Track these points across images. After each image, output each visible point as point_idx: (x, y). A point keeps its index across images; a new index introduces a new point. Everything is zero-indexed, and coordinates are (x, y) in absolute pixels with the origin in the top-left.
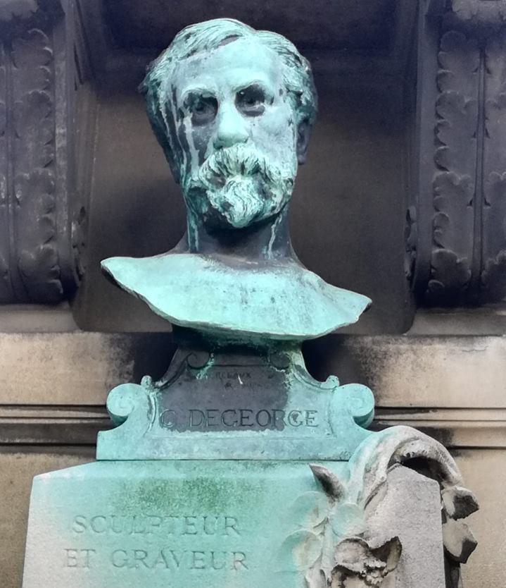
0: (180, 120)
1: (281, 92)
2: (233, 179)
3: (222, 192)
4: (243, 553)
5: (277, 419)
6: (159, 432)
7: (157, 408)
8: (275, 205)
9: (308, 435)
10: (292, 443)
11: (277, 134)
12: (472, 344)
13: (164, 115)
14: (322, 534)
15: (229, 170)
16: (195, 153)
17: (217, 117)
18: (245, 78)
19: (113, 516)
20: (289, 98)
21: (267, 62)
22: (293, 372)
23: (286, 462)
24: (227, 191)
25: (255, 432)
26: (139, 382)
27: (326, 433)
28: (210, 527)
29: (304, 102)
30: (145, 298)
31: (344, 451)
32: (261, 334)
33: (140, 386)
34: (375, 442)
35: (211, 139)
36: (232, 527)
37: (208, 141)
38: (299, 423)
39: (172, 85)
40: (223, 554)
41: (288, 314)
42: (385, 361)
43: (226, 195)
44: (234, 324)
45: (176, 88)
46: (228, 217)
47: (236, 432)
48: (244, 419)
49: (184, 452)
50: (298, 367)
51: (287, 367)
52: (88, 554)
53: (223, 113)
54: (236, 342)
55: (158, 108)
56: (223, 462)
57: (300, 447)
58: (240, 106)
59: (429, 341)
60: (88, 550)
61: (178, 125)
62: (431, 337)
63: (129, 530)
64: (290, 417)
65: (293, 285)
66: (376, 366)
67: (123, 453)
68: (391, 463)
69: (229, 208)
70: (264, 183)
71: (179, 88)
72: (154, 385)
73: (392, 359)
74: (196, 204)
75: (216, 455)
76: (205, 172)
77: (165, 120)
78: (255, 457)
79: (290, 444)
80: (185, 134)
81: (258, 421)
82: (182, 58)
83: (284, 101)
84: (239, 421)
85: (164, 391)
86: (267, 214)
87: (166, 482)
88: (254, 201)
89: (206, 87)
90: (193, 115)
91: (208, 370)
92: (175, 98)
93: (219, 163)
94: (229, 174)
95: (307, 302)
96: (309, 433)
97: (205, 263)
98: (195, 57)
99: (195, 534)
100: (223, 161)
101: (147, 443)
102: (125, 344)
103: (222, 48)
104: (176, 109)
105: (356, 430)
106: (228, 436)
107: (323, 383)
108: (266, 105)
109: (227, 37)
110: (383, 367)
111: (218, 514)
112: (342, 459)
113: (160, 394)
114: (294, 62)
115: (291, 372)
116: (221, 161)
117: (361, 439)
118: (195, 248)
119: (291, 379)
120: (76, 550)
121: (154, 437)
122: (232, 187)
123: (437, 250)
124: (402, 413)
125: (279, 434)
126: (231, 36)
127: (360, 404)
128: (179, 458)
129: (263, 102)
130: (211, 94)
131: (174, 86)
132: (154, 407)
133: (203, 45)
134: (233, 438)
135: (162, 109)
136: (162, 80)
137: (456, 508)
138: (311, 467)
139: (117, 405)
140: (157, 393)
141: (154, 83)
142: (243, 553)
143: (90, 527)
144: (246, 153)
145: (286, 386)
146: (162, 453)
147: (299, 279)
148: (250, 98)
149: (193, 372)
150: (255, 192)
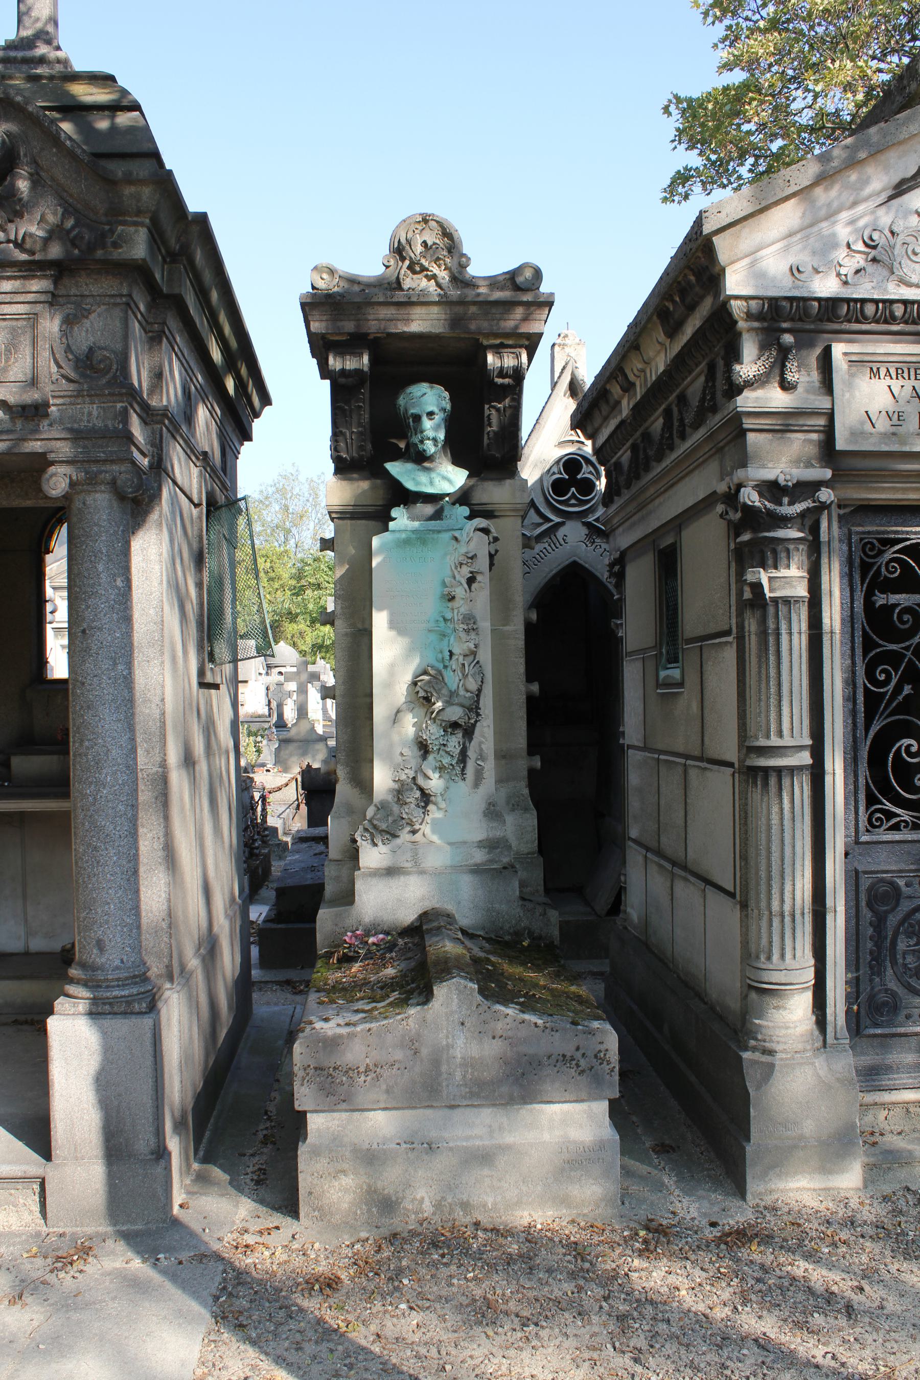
18: (430, 409)
21: (436, 403)
96: (451, 521)
148: (430, 414)
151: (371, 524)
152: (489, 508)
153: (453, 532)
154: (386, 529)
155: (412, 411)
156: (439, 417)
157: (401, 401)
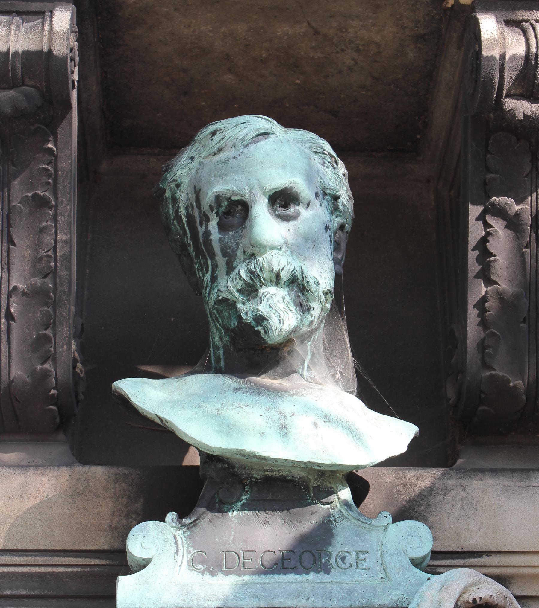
0: (204, 225)
5: (323, 560)
8: (313, 319)
9: (359, 579)
10: (341, 589)
12: (528, 478)
13: (185, 219)
15: (262, 280)
16: (221, 261)
17: (248, 221)
20: (325, 202)
25: (298, 576)
26: (163, 520)
27: (380, 577)
31: (401, 597)
33: (166, 524)
35: (241, 245)
37: (238, 248)
38: (348, 565)
39: (195, 187)
42: (431, 498)
43: (260, 308)
45: (200, 190)
46: (262, 332)
47: (276, 576)
48: (285, 561)
53: (255, 217)
54: (273, 473)
55: (177, 212)
57: (350, 592)
59: (480, 475)
61: (201, 230)
62: (483, 471)
64: (338, 560)
66: (421, 505)
69: (263, 321)
70: (300, 295)
71: (204, 189)
73: (439, 496)
74: (223, 317)
77: (185, 225)
79: (339, 589)
80: (211, 240)
82: (206, 157)
83: (321, 205)
85: (193, 529)
86: (304, 329)
89: (235, 188)
90: (220, 220)
92: (198, 200)
96: (359, 576)
98: (223, 156)
100: (256, 270)
102: (133, 479)
103: (252, 146)
104: (200, 212)
106: (267, 581)
108: (301, 209)
109: (258, 135)
110: (429, 505)
113: (188, 533)
114: (330, 163)
116: (253, 269)
118: (221, 367)
123: (488, 373)
124: (452, 558)
125: (326, 578)
126: (263, 134)
127: (417, 543)
129: (298, 205)
131: (197, 189)
133: (230, 144)
134: (272, 583)
135: (182, 211)
140: (184, 532)
145: (332, 523)
148: (283, 200)
150: (292, 304)
156: (312, 216)
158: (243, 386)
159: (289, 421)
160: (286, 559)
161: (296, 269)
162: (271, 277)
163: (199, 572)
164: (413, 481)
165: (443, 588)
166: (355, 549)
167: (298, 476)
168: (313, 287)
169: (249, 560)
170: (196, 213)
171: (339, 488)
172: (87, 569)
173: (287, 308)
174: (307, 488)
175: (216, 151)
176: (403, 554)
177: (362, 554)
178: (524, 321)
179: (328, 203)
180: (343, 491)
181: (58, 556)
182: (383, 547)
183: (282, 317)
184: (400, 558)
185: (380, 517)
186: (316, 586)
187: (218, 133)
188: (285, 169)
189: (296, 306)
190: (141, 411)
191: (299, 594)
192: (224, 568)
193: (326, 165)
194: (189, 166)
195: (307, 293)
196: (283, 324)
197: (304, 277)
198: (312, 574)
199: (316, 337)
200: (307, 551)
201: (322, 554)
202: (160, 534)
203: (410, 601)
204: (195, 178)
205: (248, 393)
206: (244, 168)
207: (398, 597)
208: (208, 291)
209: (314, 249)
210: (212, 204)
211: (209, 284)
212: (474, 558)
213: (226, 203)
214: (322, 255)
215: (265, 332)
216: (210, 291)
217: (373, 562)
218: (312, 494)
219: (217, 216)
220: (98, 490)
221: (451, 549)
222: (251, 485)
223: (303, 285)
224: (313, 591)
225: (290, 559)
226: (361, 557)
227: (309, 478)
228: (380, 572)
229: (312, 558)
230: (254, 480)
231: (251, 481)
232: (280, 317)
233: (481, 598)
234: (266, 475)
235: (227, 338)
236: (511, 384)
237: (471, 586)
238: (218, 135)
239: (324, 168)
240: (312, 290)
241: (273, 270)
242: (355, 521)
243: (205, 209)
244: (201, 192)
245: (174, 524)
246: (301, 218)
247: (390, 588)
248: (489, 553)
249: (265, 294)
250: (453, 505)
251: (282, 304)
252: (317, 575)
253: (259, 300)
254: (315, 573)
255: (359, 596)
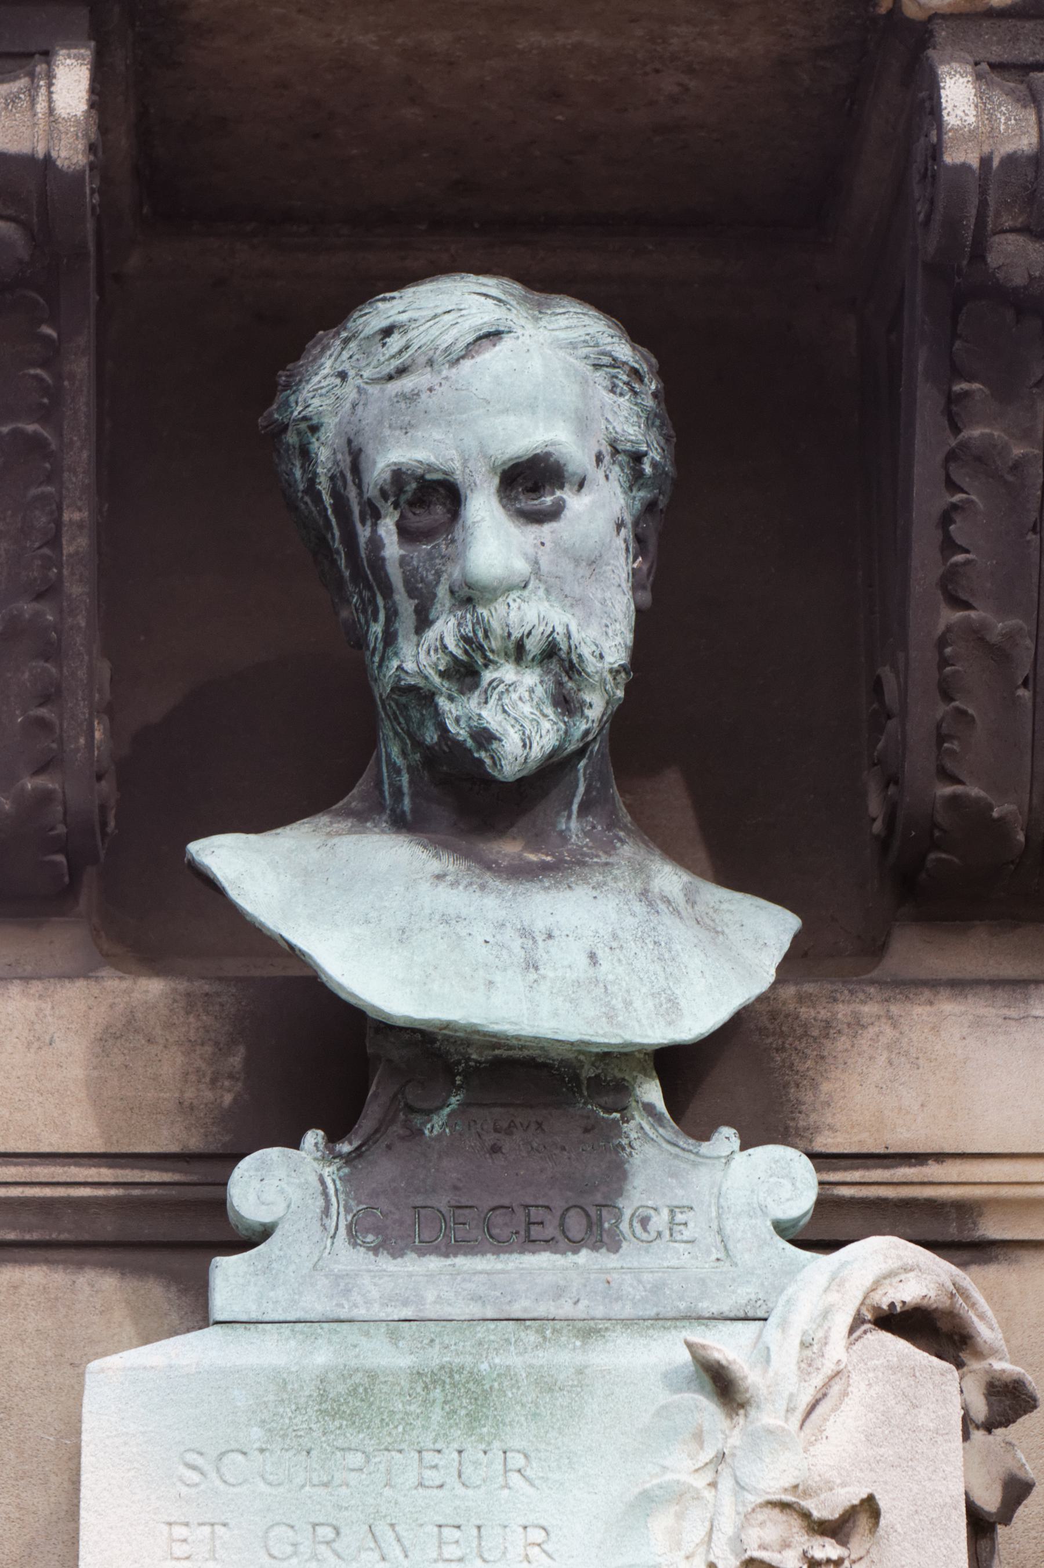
0: (369, 523)
1: (599, 458)
2: (496, 675)
3: (472, 703)
4: (544, 1529)
5: (606, 1225)
6: (350, 1258)
7: (342, 1203)
8: (590, 724)
9: (674, 1262)
10: (640, 1281)
11: (594, 563)
12: (1026, 998)
13: (327, 500)
14: (713, 1485)
15: (489, 654)
16: (406, 606)
17: (458, 526)
19: (262, 1451)
20: (617, 468)
21: (569, 394)
22: (639, 1118)
23: (628, 1323)
24: (486, 702)
25: (558, 1256)
26: (296, 1144)
27: (714, 1257)
28: (468, 1470)
29: (648, 469)
30: (310, 957)
31: (753, 1297)
32: (572, 1044)
33: (303, 1154)
34: (823, 1280)
35: (445, 576)
36: (519, 1471)
37: (438, 582)
38: (654, 1235)
39: (350, 442)
40: (500, 1530)
41: (628, 991)
43: (484, 713)
44: (511, 1023)
45: (360, 450)
46: (488, 761)
47: (515, 1256)
48: (533, 1228)
49: (405, 1303)
50: (649, 1109)
51: (625, 1108)
52: (213, 1532)
53: (474, 523)
54: (511, 1053)
55: (312, 482)
56: (492, 1325)
57: (657, 1289)
58: (508, 497)
59: (927, 994)
60: (212, 1525)
61: (364, 533)
62: (933, 984)
63: (299, 1480)
64: (635, 1224)
65: (634, 916)
66: (806, 1057)
67: (271, 1305)
68: (858, 1321)
70: (565, 679)
71: (369, 449)
72: (332, 1151)
73: (843, 1038)
74: (408, 719)
75: (475, 1310)
76: (434, 657)
77: (330, 512)
78: (561, 1313)
79: (635, 1283)
80: (383, 559)
81: (563, 1232)
82: (374, 381)
83: (607, 477)
84: (522, 1233)
85: (356, 1162)
86: (571, 748)
87: (372, 1375)
88: (546, 725)
89: (432, 459)
90: (402, 516)
91: (449, 1115)
92: (356, 469)
93: (466, 639)
94: (488, 663)
95: (667, 956)
97: (435, 866)
98: (406, 383)
99: (441, 1486)
101: (322, 1282)
102: (222, 1005)
103: (467, 365)
104: (361, 494)
105: (780, 1250)
106: (499, 1266)
107: (705, 1144)
108: (567, 495)
109: (480, 338)
110: (823, 1058)
111: (489, 1444)
112: (750, 1314)
113: (346, 1170)
114: (627, 384)
115: (633, 1118)
116: (471, 634)
117: (791, 1272)
118: (403, 812)
119: (633, 1135)
120: (187, 1524)
121: (337, 1268)
122: (495, 696)
123: (949, 790)
124: (867, 1168)
126: (488, 336)
127: (786, 1190)
128: (396, 1318)
129: (562, 487)
130: (445, 473)
132: (334, 1200)
133: (423, 359)
135: (323, 485)
136: (325, 420)
137: (990, 1404)
138: (689, 1345)
139: (252, 1198)
140: (338, 1170)
141: (303, 426)
142: (544, 1529)
143: (213, 1475)
144: (530, 614)
145: (624, 1149)
146: (355, 1306)
147: (644, 894)
148: (531, 483)
149: (417, 1120)
150: (548, 702)
151: (98, 1290)
152: (945, 1183)
153: (699, 1335)
154: (198, 1313)
155: (395, 453)
157: (329, 389)
158: (450, 867)
159: (541, 951)
160: (534, 1223)
161: (557, 629)
162: (506, 647)
163: (368, 1249)
164: (792, 1007)
165: (836, 1281)
166: (668, 1203)
167: (560, 1058)
168: (592, 665)
169: (464, 1224)
170: (352, 493)
171: (638, 1081)
172: (136, 1192)
173: (538, 713)
174: (576, 1078)
175: (393, 372)
176: (759, 1213)
177: (682, 1213)
178: (1025, 684)
179: (622, 470)
180: (646, 1086)
181: (76, 1165)
182: (721, 1200)
183: (527, 732)
184: (754, 1221)
185: (717, 1140)
186: (592, 1276)
187: (396, 331)
188: (533, 414)
189: (555, 704)
190: (248, 918)
191: (559, 1292)
192: (417, 1240)
193: (618, 391)
194: (338, 391)
195: (577, 677)
196: (530, 747)
197: (573, 647)
198: (584, 1252)
199: (596, 748)
200: (575, 1206)
201: (605, 1212)
202: (293, 1174)
203: (770, 1305)
204: (349, 423)
205: (461, 888)
206: (450, 414)
207: (747, 1298)
208: (377, 659)
209: (593, 578)
210: (386, 487)
211: (380, 646)
212: (910, 1166)
213: (414, 485)
214: (608, 588)
215: (495, 764)
216: (382, 660)
217: (702, 1229)
218: (586, 1094)
219: (395, 508)
220: (153, 1028)
221: (864, 1150)
222: (467, 1075)
223: (571, 661)
224: (585, 1286)
225: (542, 1223)
226: (680, 1218)
227: (580, 1061)
228: (716, 1247)
229: (584, 1221)
230: (472, 1064)
231: (467, 1066)
232: (524, 734)
233: (904, 1303)
234: (496, 1057)
235: (418, 756)
236: (995, 814)
237: (886, 1277)
238: (396, 336)
239: (615, 398)
240: (589, 670)
241: (509, 635)
242: (669, 1147)
243: (369, 495)
244: (363, 456)
245: (319, 1154)
246: (567, 513)
247: (734, 1280)
248: (940, 1157)
249: (495, 684)
250: (870, 1058)
251: (528, 704)
252: (594, 1254)
253: (483, 697)
254: (589, 1251)
255: (674, 1296)
